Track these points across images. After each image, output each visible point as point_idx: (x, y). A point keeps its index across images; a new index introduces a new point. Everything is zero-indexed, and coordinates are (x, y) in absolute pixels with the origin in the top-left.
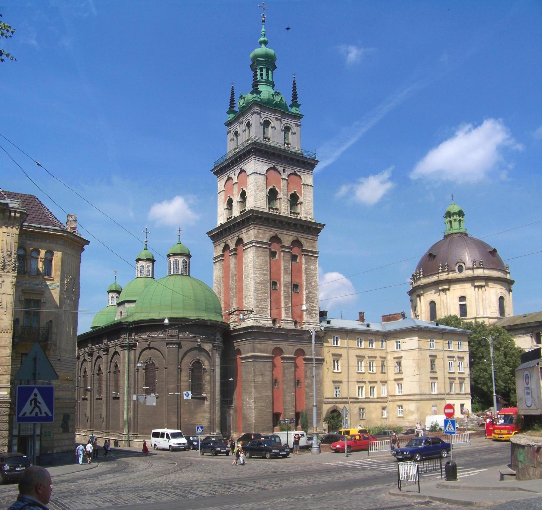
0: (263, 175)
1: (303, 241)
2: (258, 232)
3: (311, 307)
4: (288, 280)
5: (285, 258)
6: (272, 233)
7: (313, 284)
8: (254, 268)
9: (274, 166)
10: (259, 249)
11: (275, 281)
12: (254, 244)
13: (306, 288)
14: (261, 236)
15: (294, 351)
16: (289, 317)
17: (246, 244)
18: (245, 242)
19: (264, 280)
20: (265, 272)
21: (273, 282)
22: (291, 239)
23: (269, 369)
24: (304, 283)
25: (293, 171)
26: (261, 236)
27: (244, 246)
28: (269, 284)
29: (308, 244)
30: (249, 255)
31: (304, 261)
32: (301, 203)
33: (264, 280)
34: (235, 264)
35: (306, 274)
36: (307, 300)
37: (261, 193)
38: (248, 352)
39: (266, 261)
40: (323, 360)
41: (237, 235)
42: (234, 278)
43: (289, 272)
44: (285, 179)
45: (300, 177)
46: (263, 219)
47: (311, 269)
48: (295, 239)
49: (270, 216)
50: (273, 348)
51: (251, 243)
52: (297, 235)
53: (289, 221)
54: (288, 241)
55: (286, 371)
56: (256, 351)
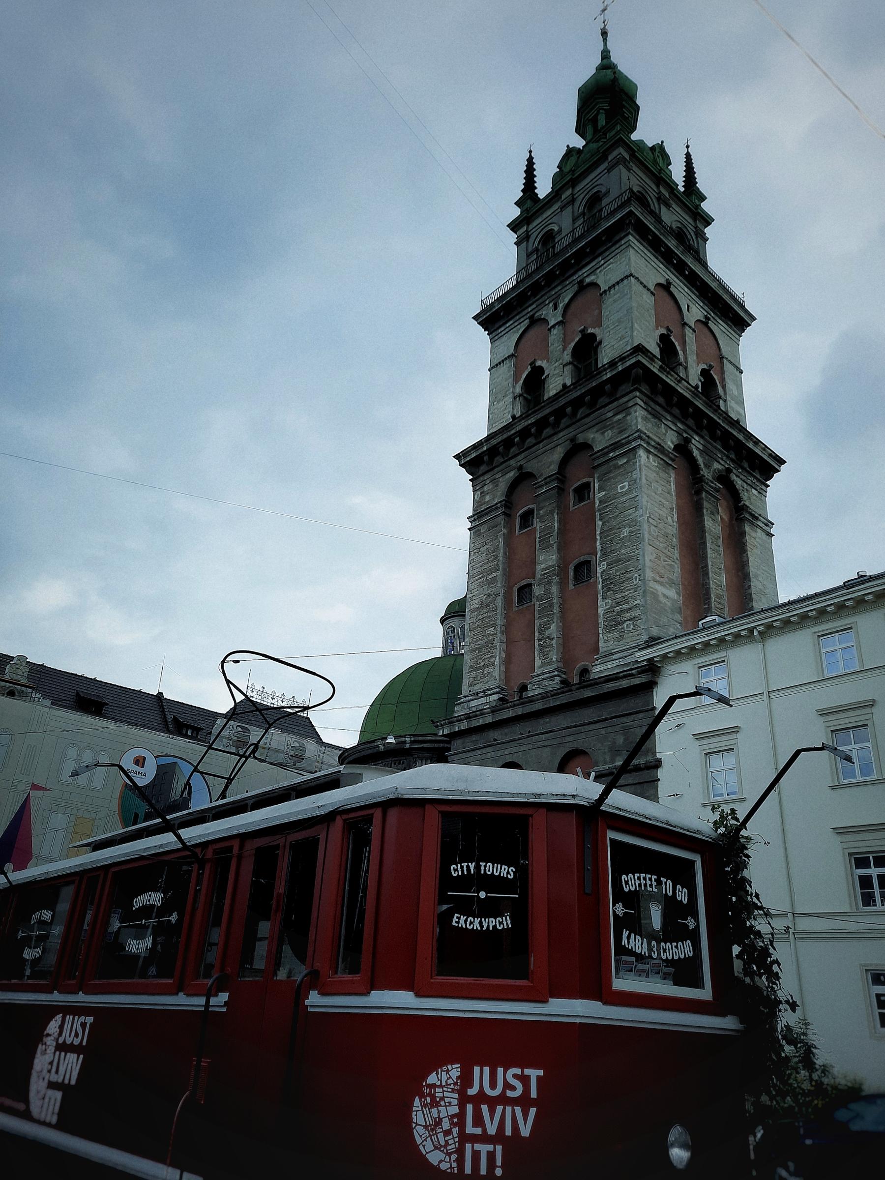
0: (506, 359)
3: (619, 604)
7: (625, 532)
9: (530, 318)
13: (601, 557)
14: (487, 498)
16: (550, 663)
19: (489, 595)
21: (521, 589)
22: (558, 454)
24: (598, 544)
25: (576, 288)
28: (499, 601)
29: (609, 434)
31: (597, 485)
32: (600, 342)
36: (607, 588)
37: (501, 403)
39: (496, 549)
40: (658, 764)
43: (553, 540)
44: (554, 326)
45: (594, 285)
46: (486, 458)
48: (568, 445)
49: (494, 442)
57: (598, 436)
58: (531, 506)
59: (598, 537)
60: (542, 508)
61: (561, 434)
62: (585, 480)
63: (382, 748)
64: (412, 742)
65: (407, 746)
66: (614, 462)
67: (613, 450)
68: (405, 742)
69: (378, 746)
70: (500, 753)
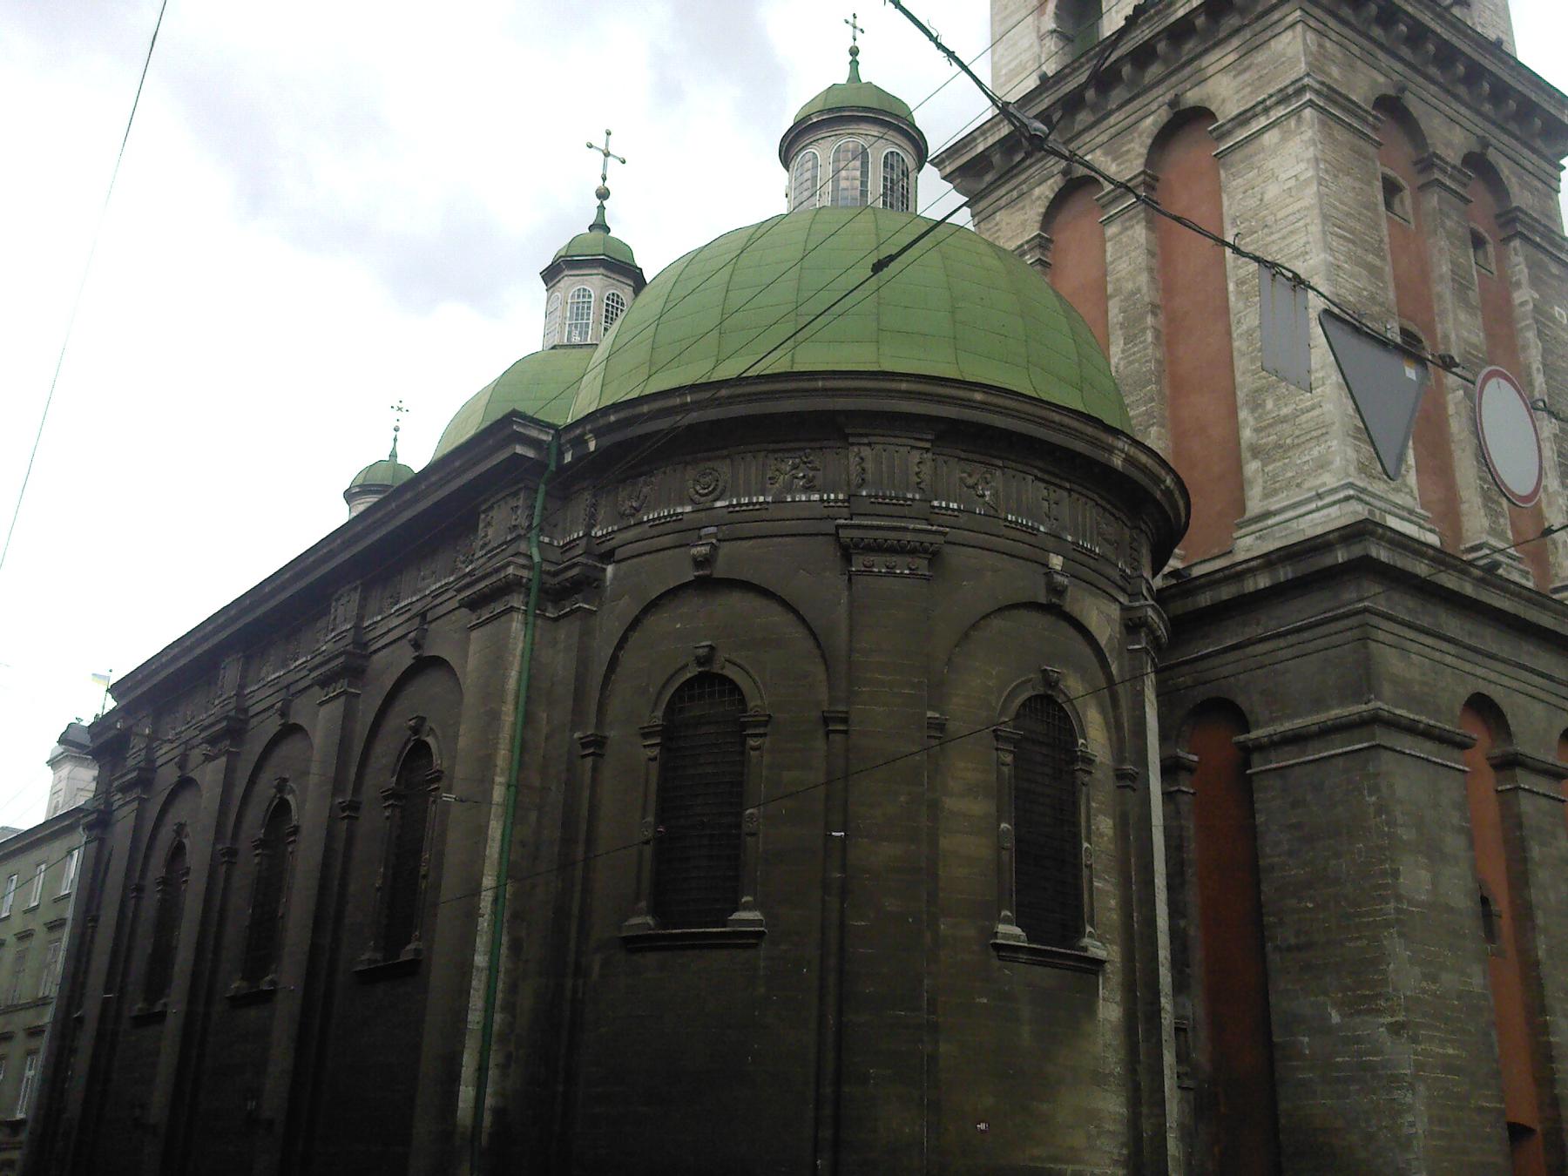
1: (1505, 168)
2: (1320, 46)
4: (1474, 339)
5: (1448, 223)
6: (1381, 79)
8: (1326, 218)
10: (1341, 134)
11: (1413, 328)
12: (1308, 96)
14: (1335, 72)
15: (1556, 735)
16: (1501, 535)
17: (1243, 118)
18: (1232, 110)
20: (1370, 258)
23: (1455, 818)
26: (1335, 72)
27: (1222, 137)
30: (1271, 164)
33: (1372, 298)
34: (1151, 254)
35: (1540, 334)
38: (1319, 704)
41: (1169, 96)
42: (1150, 320)
43: (1474, 296)
47: (1552, 318)
50: (1464, 693)
51: (1284, 99)
52: (1481, 127)
53: (1455, 41)
54: (1449, 144)
55: (1536, 852)
56: (1387, 689)
57: (1514, 180)
58: (1403, 182)
59: (1536, 364)
60: (1448, 217)
61: (1463, 110)
62: (1481, 230)
63: (1118, 462)
64: (1168, 492)
65: (1158, 495)
66: (1546, 259)
67: (1542, 236)
68: (1158, 480)
69: (1110, 450)
70: (1468, 667)
